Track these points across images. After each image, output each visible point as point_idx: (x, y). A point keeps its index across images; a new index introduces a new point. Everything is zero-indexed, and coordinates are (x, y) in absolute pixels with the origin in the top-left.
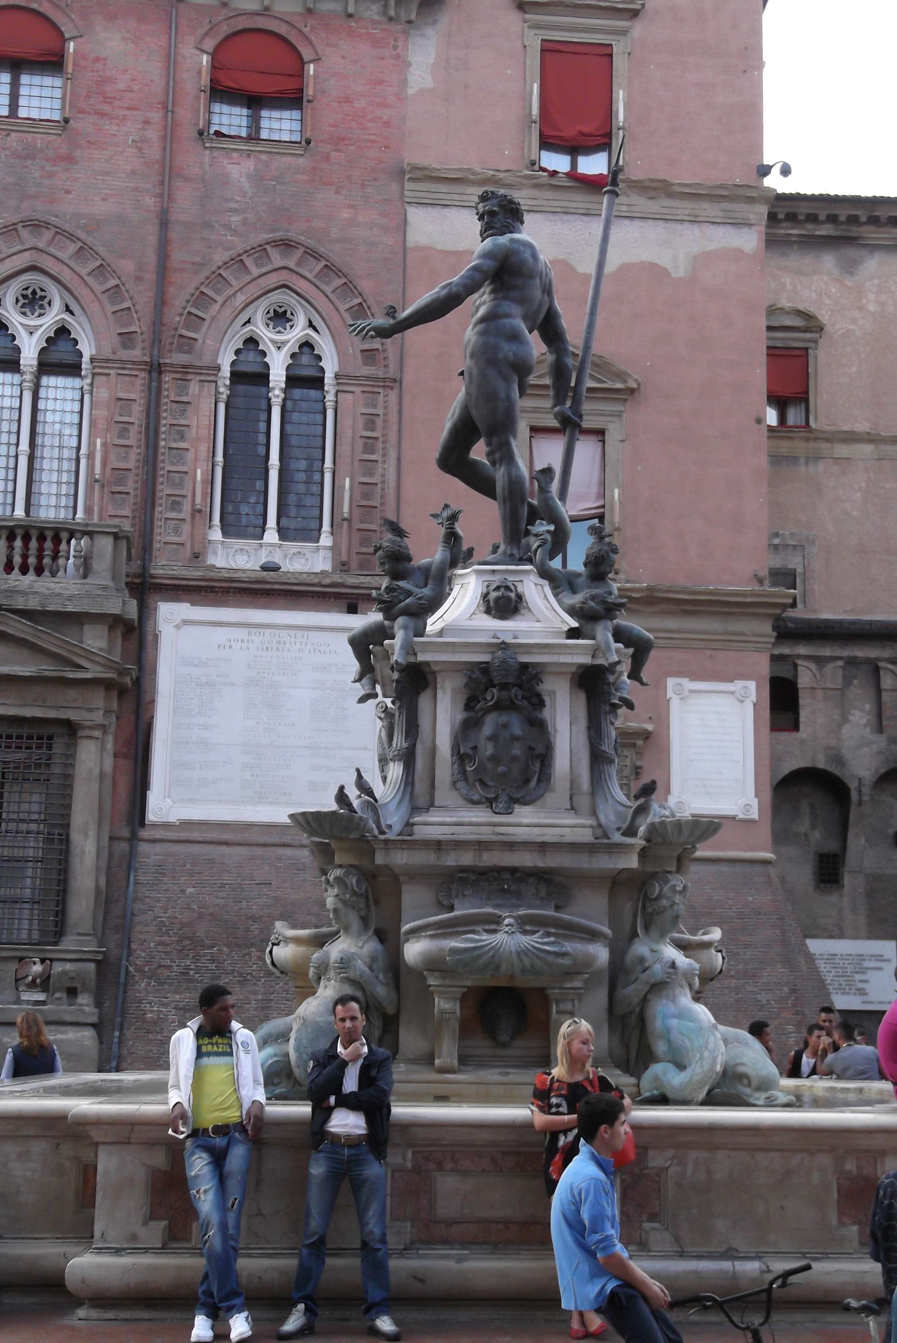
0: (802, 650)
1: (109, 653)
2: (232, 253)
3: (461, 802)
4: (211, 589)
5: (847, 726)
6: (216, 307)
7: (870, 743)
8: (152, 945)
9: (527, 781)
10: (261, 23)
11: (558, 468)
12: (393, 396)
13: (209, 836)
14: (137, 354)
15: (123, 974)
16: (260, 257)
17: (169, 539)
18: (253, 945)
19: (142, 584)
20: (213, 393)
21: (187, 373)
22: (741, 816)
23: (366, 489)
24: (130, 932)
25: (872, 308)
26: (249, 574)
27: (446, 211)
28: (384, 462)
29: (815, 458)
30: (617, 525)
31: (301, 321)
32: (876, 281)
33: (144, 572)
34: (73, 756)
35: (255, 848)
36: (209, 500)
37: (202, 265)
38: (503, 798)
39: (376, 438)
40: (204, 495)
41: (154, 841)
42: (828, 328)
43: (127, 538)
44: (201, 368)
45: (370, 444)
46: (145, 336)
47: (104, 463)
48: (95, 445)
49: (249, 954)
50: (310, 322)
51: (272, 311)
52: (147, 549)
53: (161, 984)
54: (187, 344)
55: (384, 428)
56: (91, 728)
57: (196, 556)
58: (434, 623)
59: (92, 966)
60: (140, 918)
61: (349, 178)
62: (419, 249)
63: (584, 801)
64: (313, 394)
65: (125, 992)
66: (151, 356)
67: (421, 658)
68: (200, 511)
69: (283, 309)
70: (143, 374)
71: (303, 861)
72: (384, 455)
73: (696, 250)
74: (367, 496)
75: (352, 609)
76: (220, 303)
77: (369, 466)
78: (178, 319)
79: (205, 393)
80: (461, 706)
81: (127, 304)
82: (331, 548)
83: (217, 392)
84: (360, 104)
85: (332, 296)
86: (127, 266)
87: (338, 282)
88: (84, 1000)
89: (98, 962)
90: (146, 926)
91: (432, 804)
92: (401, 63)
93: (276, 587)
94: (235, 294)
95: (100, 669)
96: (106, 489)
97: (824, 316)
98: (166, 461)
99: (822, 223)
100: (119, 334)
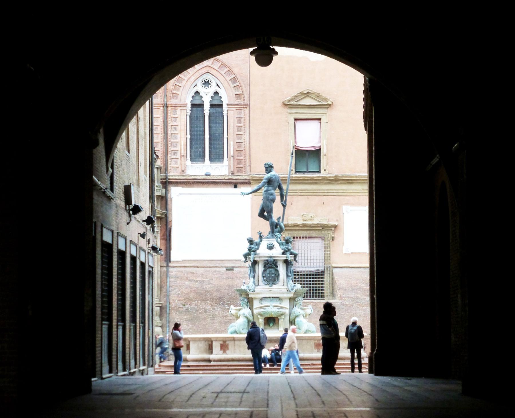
3: (264, 285)
4: (189, 182)
6: (184, 82)
8: (176, 301)
9: (275, 280)
12: (247, 110)
13: (192, 265)
15: (168, 310)
17: (173, 166)
18: (208, 300)
19: (165, 182)
21: (176, 106)
24: (169, 297)
26: (201, 177)
30: (325, 154)
31: (213, 84)
33: (166, 177)
35: (207, 268)
36: (186, 151)
38: (271, 284)
39: (242, 126)
40: (184, 150)
41: (174, 267)
43: (161, 168)
44: (181, 105)
46: (161, 94)
49: (207, 303)
50: (217, 84)
51: (204, 81)
52: (166, 169)
55: (244, 123)
57: (183, 171)
58: (258, 252)
60: (172, 292)
63: (285, 284)
64: (219, 109)
65: (169, 316)
67: (256, 259)
68: (183, 156)
69: (207, 80)
70: (162, 108)
71: (223, 272)
74: (239, 147)
75: (236, 187)
76: (186, 80)
78: (172, 87)
80: (263, 267)
83: (187, 112)
85: (224, 75)
89: (160, 307)
90: (174, 295)
91: (258, 285)
93: (210, 181)
98: (171, 138)
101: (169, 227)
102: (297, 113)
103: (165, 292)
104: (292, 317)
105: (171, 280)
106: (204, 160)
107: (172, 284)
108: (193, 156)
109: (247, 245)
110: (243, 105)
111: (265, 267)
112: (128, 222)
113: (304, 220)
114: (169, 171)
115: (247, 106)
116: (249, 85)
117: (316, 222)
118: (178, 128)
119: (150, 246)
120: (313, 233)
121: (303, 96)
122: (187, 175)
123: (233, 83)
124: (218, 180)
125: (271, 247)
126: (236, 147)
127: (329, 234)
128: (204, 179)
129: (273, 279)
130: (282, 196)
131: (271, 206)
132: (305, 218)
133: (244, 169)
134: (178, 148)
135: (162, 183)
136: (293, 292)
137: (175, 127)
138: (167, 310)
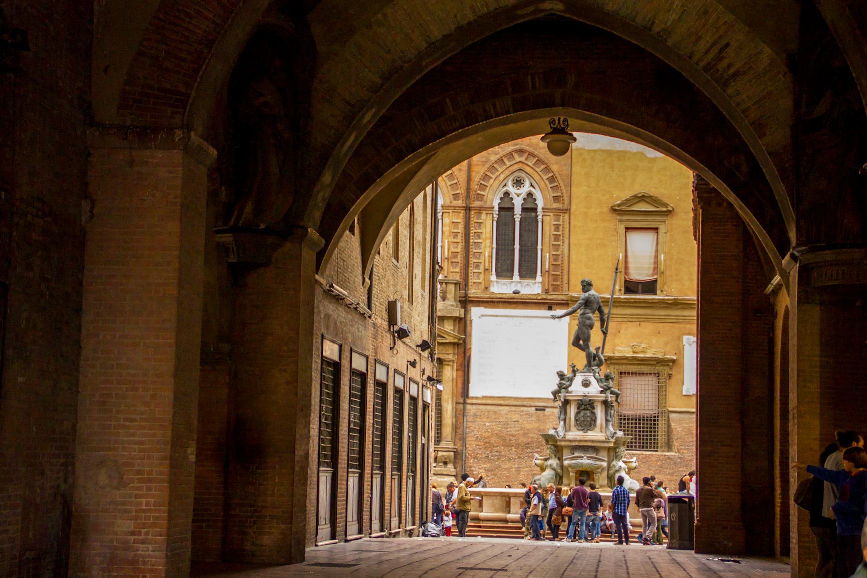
1: (454, 332)
2: (498, 156)
4: (492, 302)
6: (492, 181)
11: (601, 345)
12: (566, 216)
14: (459, 203)
15: (464, 457)
16: (510, 158)
17: (475, 281)
18: (513, 446)
19: (465, 300)
20: (491, 218)
23: (555, 257)
26: (508, 295)
28: (563, 245)
31: (527, 183)
33: (466, 295)
34: (441, 372)
35: (512, 407)
37: (486, 162)
39: (559, 235)
40: (489, 262)
45: (557, 238)
46: (463, 195)
47: (448, 250)
48: (444, 242)
50: (531, 184)
52: (466, 285)
53: (478, 461)
54: (480, 197)
55: (563, 231)
56: (449, 361)
58: (570, 389)
59: (452, 453)
60: (469, 435)
63: (604, 430)
64: (533, 214)
66: (466, 203)
67: (567, 398)
68: (487, 270)
70: (463, 211)
72: (563, 242)
75: (550, 308)
76: (494, 179)
77: (556, 247)
79: (488, 218)
81: (455, 181)
82: (541, 283)
83: (493, 217)
85: (540, 173)
87: (543, 167)
88: (450, 466)
89: (454, 452)
91: (570, 430)
94: (499, 175)
95: (451, 338)
96: (449, 261)
100: (453, 194)
101: (467, 355)
102: (628, 220)
103: (460, 435)
104: (611, 472)
105: (468, 419)
106: (513, 275)
107: (470, 424)
108: (499, 270)
109: (557, 380)
110: (563, 210)
111: (578, 409)
112: (392, 346)
113: (634, 352)
114: (470, 287)
116: (571, 186)
117: (649, 355)
118: (483, 236)
119: (425, 377)
120: (645, 369)
121: (637, 200)
122: (492, 293)
123: (551, 182)
124: (529, 299)
125: (586, 384)
126: (551, 260)
127: (665, 371)
128: (511, 299)
129: (588, 423)
130: (602, 321)
131: (588, 333)
132: (635, 350)
133: (562, 287)
135: (460, 301)
136: (613, 440)
137: (478, 235)
138: (462, 456)
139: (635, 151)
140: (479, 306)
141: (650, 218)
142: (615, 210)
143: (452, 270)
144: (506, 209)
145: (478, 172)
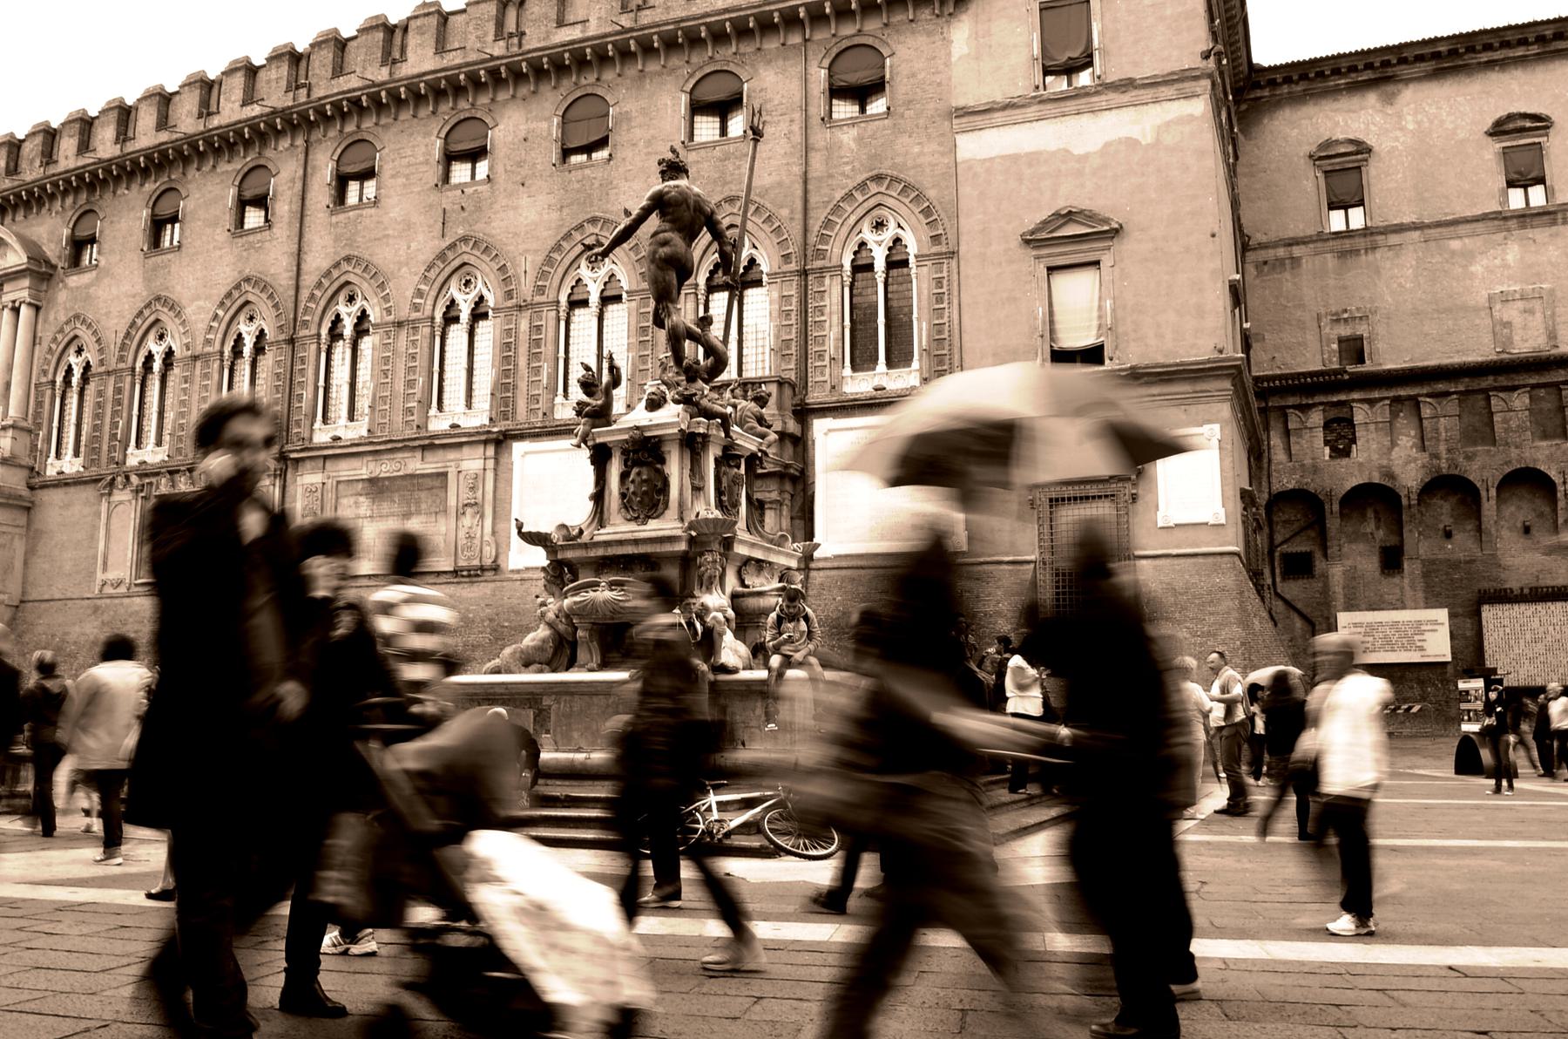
0: (1356, 396)
2: (847, 190)
4: (844, 408)
5: (1396, 449)
7: (1415, 460)
10: (857, 40)
12: (954, 263)
14: (793, 266)
22: (1211, 522)
25: (1411, 127)
27: (981, 132)
29: (1374, 248)
31: (892, 225)
32: (1412, 106)
37: (828, 202)
41: (819, 569)
42: (1376, 149)
45: (939, 298)
54: (821, 254)
61: (917, 126)
62: (963, 162)
73: (1159, 121)
74: (940, 332)
77: (939, 312)
84: (920, 77)
86: (785, 212)
92: (947, 42)
97: (1371, 141)
99: (1362, 71)
102: (1049, 256)
115: (952, 254)
118: (827, 310)
123: (927, 217)
134: (826, 348)
139: (1054, 149)
140: (825, 416)
141: (1085, 247)
142: (1027, 242)
143: (784, 367)
144: (862, 268)
145: (817, 219)
